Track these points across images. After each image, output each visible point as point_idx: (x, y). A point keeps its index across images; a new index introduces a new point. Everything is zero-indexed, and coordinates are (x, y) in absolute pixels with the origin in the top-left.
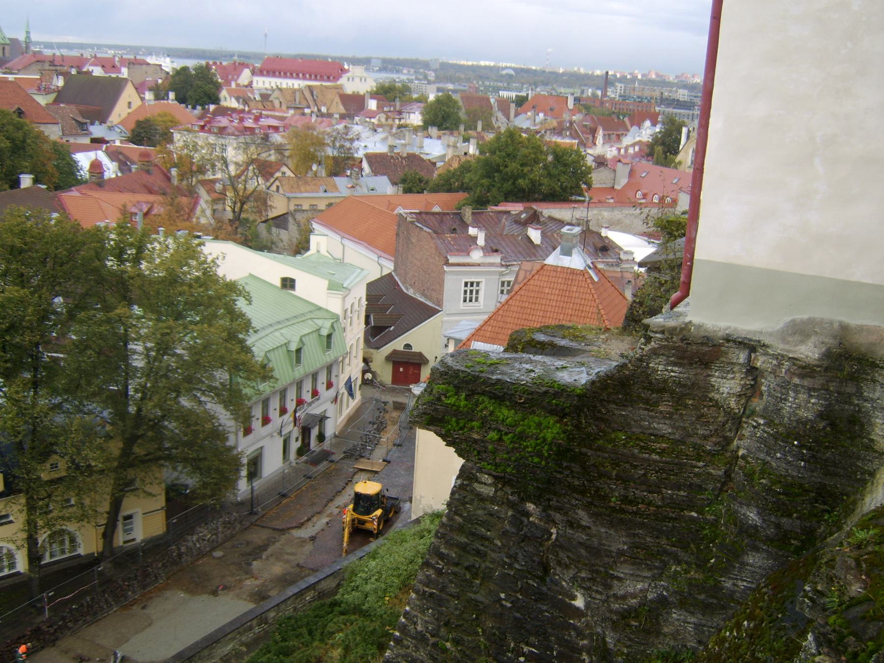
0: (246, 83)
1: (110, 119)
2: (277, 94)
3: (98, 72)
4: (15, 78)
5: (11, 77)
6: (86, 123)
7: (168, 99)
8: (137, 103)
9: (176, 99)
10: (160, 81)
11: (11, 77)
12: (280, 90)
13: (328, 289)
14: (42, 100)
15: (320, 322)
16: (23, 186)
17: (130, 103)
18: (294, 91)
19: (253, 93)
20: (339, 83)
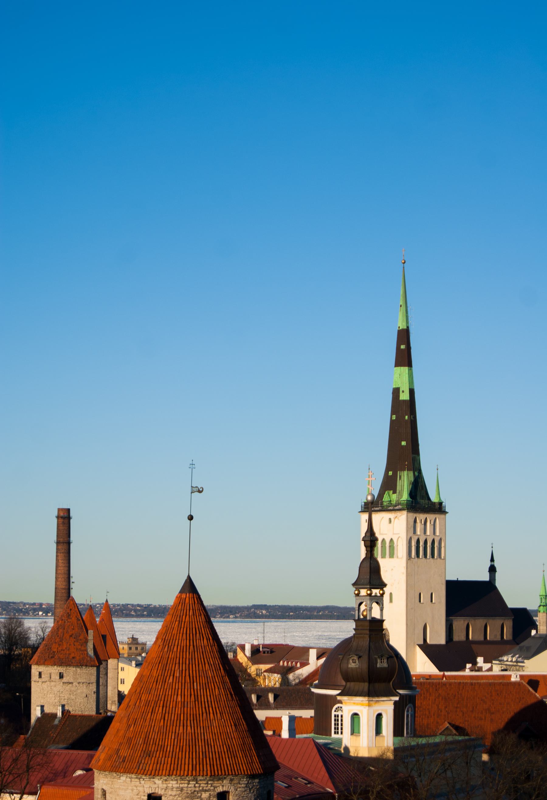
4: (522, 677)
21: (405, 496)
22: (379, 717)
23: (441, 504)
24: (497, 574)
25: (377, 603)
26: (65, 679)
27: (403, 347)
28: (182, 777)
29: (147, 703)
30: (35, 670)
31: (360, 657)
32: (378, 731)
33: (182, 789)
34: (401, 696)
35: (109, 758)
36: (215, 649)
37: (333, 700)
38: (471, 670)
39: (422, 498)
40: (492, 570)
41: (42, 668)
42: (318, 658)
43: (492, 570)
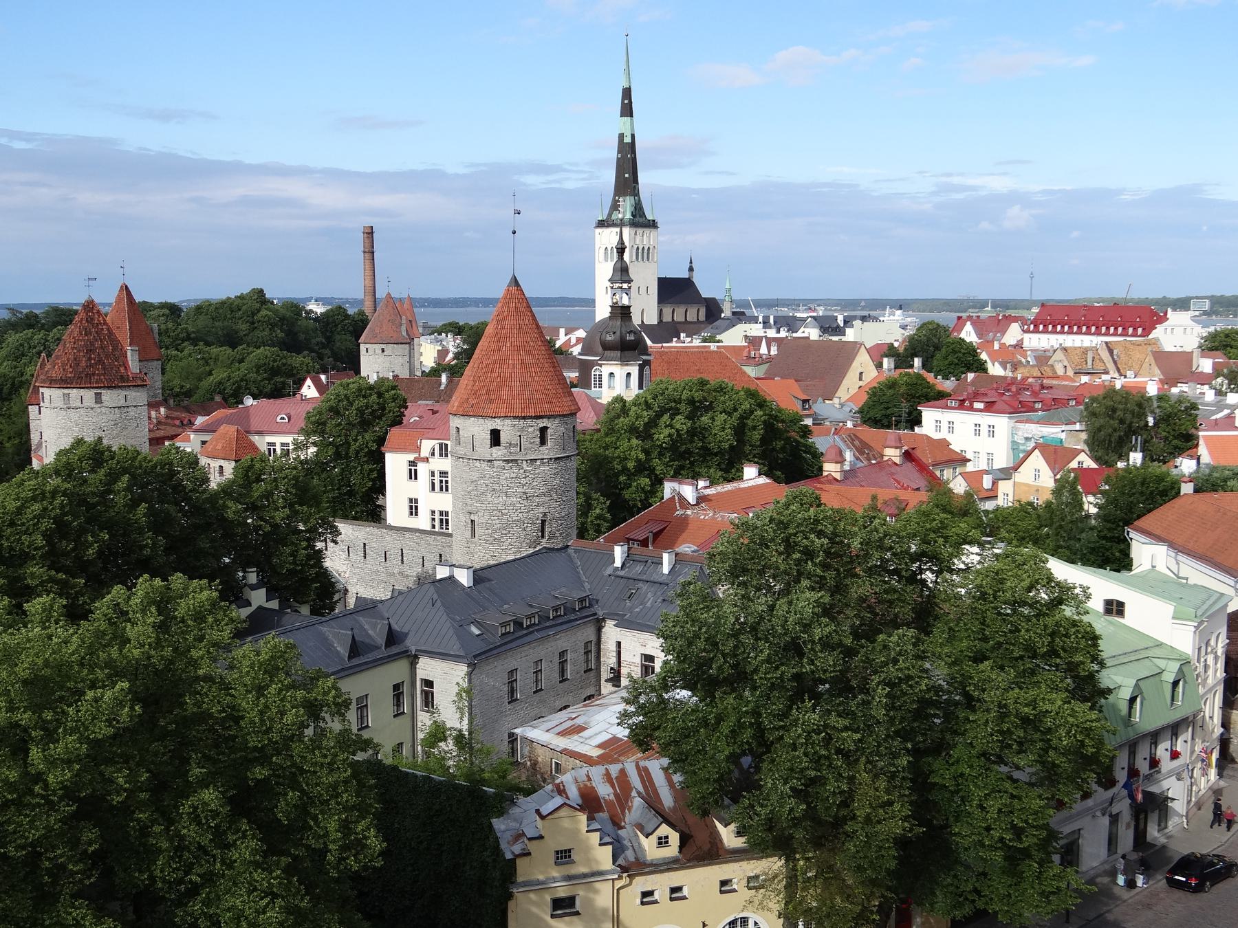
0: (1014, 342)
1: (836, 395)
2: (1059, 355)
3: (813, 333)
5: (713, 346)
6: (808, 400)
7: (912, 366)
8: (871, 374)
9: (924, 366)
10: (896, 344)
11: (713, 346)
12: (1065, 349)
13: (1174, 618)
14: (751, 371)
15: (1162, 664)
16: (745, 478)
17: (861, 373)
18: (1085, 351)
19: (1025, 357)
20: (1151, 337)
21: (628, 216)
22: (629, 374)
23: (654, 221)
24: (695, 275)
25: (627, 294)
26: (385, 353)
27: (626, 102)
28: (515, 417)
29: (487, 366)
30: (362, 347)
31: (614, 333)
32: (628, 386)
33: (515, 426)
34: (644, 361)
35: (460, 405)
36: (534, 326)
37: (593, 363)
38: (676, 342)
39: (641, 216)
40: (691, 269)
41: (368, 346)
42: (566, 335)
43: (691, 269)
